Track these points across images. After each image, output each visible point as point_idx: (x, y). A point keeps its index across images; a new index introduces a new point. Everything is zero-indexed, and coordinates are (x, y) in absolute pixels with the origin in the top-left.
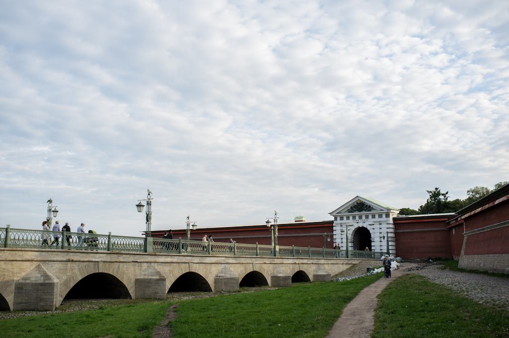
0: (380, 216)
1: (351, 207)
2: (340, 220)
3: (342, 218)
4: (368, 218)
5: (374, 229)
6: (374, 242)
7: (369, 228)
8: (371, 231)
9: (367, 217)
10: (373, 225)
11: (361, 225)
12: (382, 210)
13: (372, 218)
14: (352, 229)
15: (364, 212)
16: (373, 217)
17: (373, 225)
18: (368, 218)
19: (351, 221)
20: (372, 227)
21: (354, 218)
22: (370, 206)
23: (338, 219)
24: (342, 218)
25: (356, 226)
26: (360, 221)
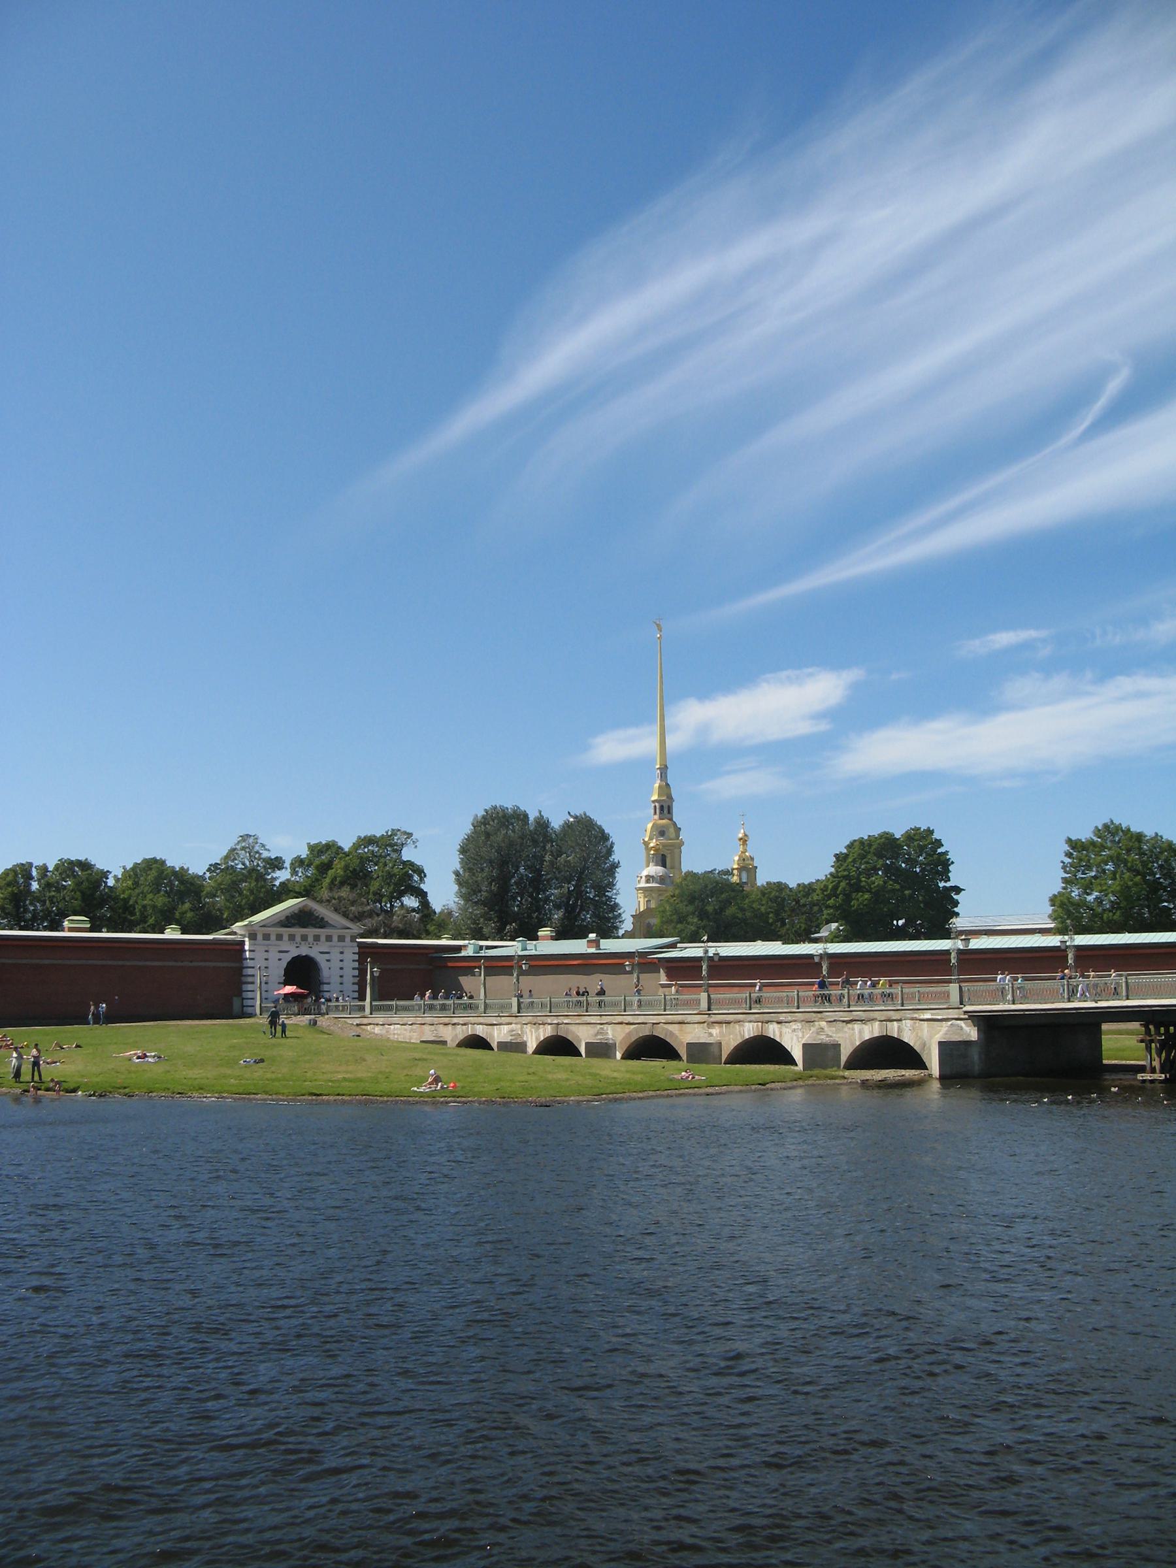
0: (341, 939)
1: (287, 917)
2: (264, 939)
3: (266, 937)
4: (319, 941)
5: (328, 961)
6: (329, 984)
7: (321, 959)
8: (323, 965)
9: (317, 938)
10: (328, 953)
11: (304, 951)
12: (348, 928)
13: (327, 940)
14: (288, 958)
15: (311, 932)
16: (329, 938)
17: (328, 953)
18: (319, 941)
19: (285, 945)
20: (327, 956)
21: (292, 938)
22: (322, 918)
23: (260, 937)
24: (266, 937)
25: (295, 952)
26: (303, 943)
